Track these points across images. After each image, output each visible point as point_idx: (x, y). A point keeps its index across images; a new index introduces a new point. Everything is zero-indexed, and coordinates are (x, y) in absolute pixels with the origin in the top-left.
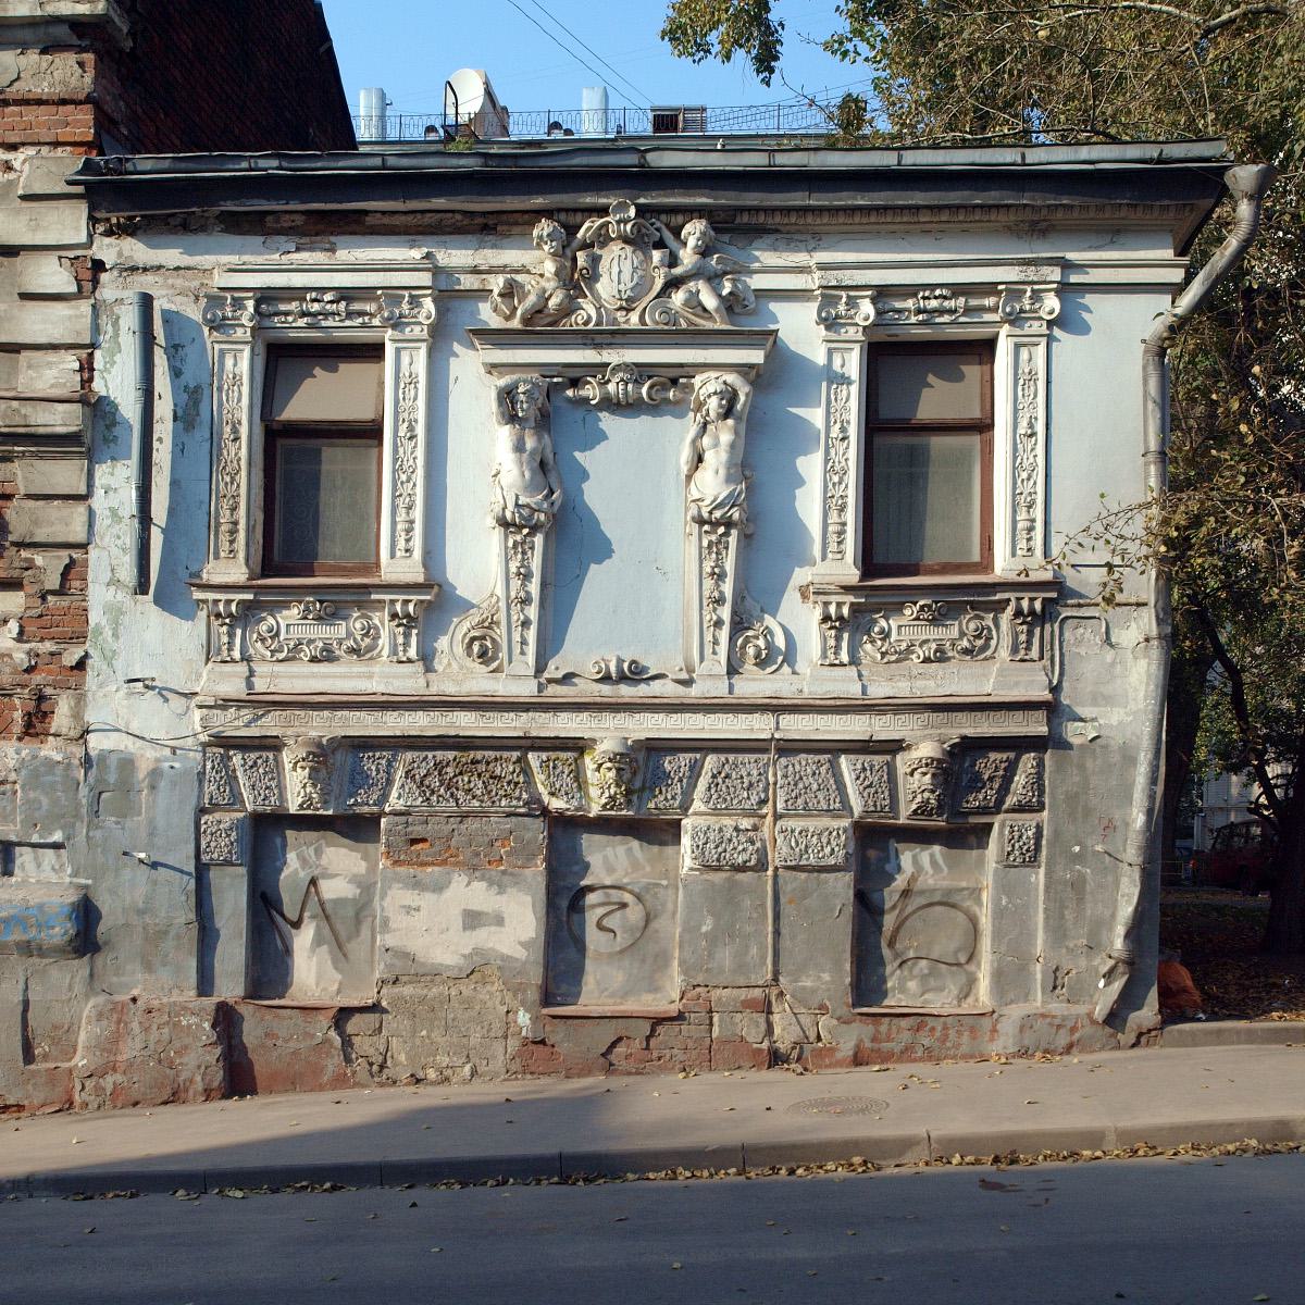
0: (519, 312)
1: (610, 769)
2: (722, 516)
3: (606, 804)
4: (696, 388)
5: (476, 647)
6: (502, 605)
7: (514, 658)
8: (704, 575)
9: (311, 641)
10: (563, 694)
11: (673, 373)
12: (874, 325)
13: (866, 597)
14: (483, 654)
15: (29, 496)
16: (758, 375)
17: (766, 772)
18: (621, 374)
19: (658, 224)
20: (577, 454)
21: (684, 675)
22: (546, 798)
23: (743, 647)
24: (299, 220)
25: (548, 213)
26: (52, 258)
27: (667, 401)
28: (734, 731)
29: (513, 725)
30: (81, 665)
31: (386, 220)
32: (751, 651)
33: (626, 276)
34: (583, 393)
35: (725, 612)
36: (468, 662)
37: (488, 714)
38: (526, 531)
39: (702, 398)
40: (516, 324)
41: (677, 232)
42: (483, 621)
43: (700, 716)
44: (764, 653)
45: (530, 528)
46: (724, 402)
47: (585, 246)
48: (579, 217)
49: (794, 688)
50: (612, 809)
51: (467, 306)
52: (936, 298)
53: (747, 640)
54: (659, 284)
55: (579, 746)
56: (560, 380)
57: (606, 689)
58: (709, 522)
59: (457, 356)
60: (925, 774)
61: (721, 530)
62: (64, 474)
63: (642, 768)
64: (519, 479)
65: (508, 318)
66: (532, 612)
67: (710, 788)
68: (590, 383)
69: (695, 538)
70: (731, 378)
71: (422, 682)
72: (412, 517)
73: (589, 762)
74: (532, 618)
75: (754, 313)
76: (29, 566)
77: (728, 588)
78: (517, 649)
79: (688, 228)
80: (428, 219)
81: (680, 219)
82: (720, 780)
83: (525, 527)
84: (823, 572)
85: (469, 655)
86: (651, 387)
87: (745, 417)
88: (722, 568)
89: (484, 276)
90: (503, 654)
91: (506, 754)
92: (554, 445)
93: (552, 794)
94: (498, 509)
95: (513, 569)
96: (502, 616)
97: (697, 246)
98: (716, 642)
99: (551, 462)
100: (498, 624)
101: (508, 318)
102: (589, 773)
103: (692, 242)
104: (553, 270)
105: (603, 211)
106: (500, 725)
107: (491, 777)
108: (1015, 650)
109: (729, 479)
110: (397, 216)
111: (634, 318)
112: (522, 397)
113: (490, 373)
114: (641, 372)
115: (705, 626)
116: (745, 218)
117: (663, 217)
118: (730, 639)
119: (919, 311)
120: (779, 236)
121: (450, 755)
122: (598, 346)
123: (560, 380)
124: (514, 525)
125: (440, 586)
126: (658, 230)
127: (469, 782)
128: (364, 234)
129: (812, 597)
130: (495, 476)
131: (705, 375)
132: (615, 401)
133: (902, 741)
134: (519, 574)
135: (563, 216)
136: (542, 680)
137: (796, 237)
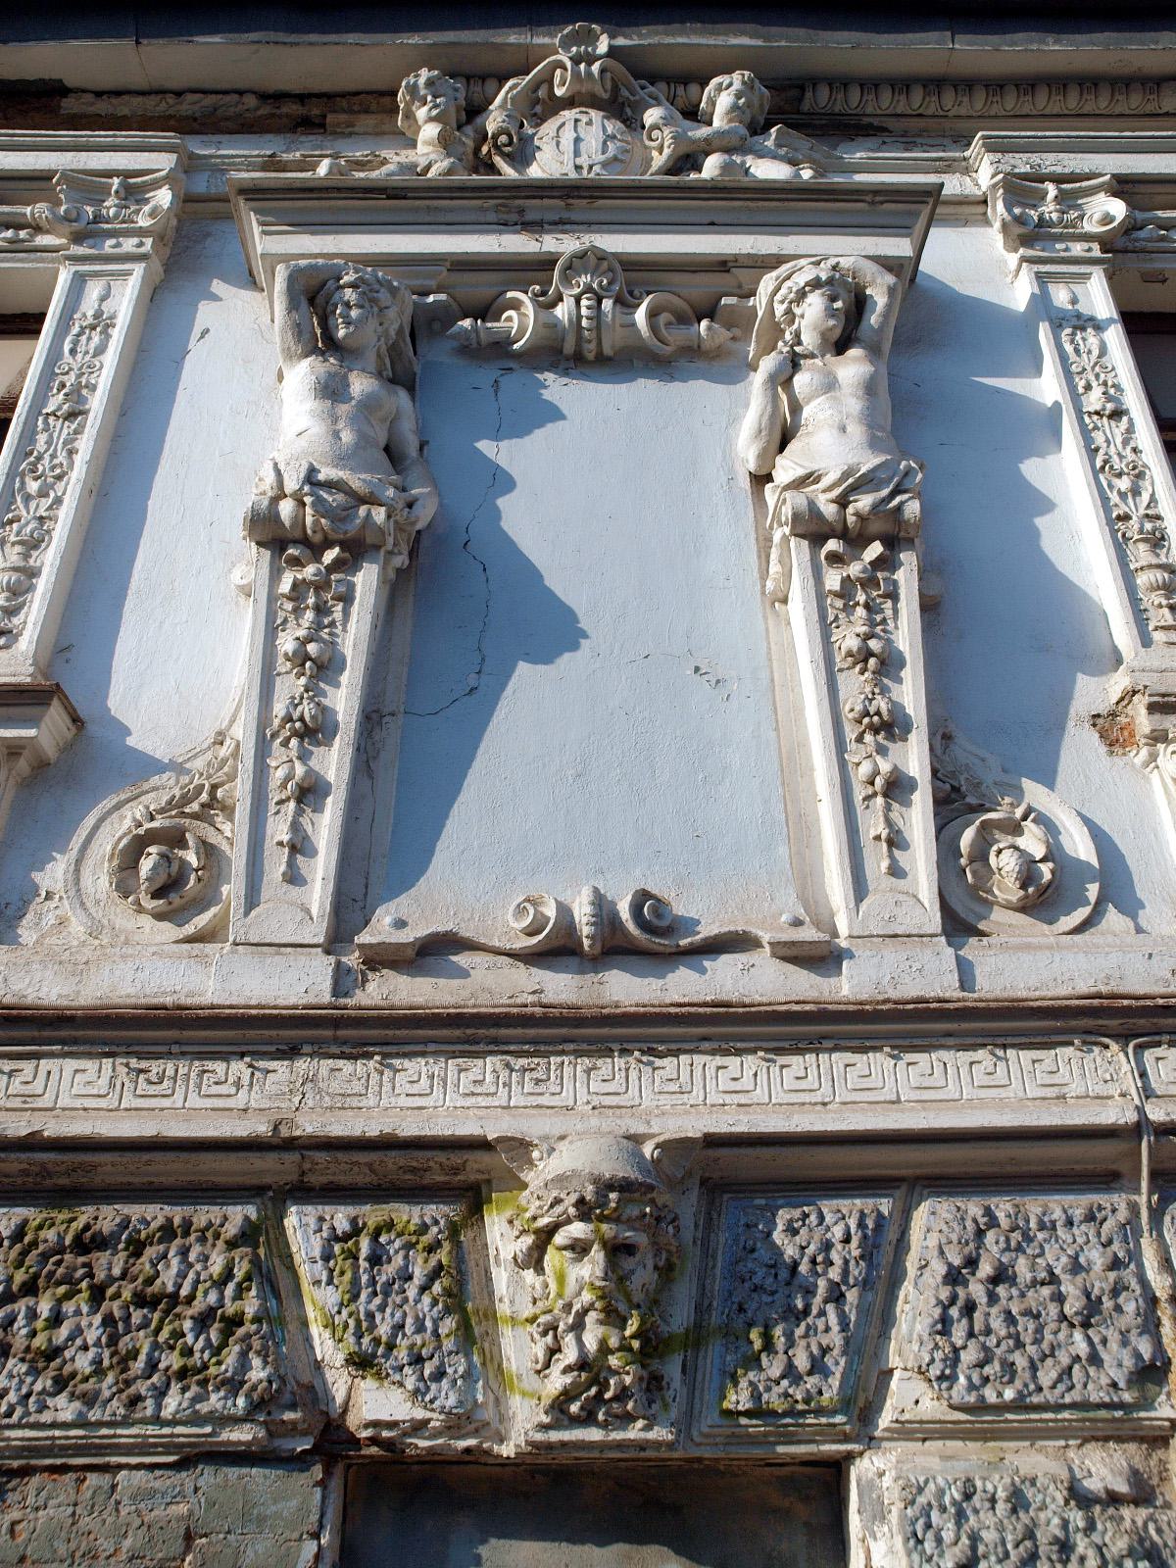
1: (579, 1249)
2: (875, 507)
3: (567, 1395)
7: (265, 893)
8: (839, 661)
11: (699, 287)
14: (167, 887)
17: (1135, 1255)
18: (584, 279)
20: (485, 446)
22: (339, 1383)
23: (980, 855)
28: (1001, 1104)
31: (102, 107)
35: (914, 757)
36: (122, 916)
37: (155, 1067)
38: (330, 556)
42: (186, 799)
43: (878, 1063)
44: (1046, 870)
45: (344, 545)
46: (839, 304)
50: (587, 1419)
56: (443, 297)
57: (560, 987)
59: (216, 298)
61: (875, 550)
63: (694, 1253)
66: (334, 762)
67: (944, 1326)
68: (516, 305)
74: (331, 776)
77: (910, 693)
78: (276, 865)
82: (977, 1290)
83: (328, 544)
85: (124, 889)
87: (887, 346)
90: (232, 890)
91: (204, 1215)
92: (421, 430)
93: (362, 1363)
95: (286, 644)
96: (240, 791)
97: (735, 107)
98: (895, 841)
99: (412, 449)
106: (194, 1101)
107: (140, 1300)
110: (126, 97)
112: (349, 294)
114: (635, 276)
115: (859, 793)
118: (939, 830)
120: (887, 140)
123: (443, 297)
124: (304, 541)
127: (56, 1320)
132: (569, 347)
134: (300, 658)
136: (352, 960)
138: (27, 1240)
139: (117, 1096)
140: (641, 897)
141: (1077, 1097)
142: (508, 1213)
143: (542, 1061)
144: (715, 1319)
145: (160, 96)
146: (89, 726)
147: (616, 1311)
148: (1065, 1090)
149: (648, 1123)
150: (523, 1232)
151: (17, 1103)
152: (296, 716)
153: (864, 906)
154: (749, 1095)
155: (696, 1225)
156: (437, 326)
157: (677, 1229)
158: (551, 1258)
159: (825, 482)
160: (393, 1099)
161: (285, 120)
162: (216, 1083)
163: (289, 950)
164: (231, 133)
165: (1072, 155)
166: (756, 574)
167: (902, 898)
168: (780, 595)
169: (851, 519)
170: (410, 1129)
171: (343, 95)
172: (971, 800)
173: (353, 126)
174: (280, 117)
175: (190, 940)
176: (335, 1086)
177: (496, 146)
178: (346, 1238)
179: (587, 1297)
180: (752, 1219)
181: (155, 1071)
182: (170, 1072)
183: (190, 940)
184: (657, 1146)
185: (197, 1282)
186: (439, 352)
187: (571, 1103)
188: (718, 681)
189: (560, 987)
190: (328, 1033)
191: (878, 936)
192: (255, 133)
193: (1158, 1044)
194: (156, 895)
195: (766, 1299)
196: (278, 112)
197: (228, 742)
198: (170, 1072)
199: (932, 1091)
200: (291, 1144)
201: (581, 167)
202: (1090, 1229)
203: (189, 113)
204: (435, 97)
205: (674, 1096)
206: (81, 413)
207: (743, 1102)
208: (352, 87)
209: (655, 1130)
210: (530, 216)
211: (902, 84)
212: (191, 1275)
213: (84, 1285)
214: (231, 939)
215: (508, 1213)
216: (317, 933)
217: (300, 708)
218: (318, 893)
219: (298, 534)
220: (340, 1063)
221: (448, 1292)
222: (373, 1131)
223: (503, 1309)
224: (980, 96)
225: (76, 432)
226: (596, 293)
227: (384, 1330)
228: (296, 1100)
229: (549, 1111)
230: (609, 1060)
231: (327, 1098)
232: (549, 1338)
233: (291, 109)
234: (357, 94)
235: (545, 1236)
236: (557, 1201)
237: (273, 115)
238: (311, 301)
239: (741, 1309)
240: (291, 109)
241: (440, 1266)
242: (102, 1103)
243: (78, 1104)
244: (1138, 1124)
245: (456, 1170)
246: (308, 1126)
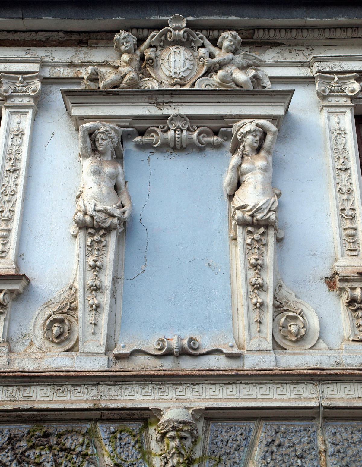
5: (55, 330)
10: (130, 369)
11: (215, 124)
21: (236, 351)
28: (283, 400)
29: (85, 398)
31: (11, 37)
39: (239, 138)
42: (63, 308)
48: (145, 32)
49: (333, 361)
56: (131, 129)
57: (168, 364)
66: (104, 300)
70: (261, 122)
72: (10, 228)
73: (153, 434)
81: (216, 33)
86: (199, 134)
89: (77, 69)
91: (76, 426)
100: (75, 309)
102: (153, 444)
106: (73, 398)
107: (62, 450)
110: (18, 33)
116: (260, 34)
120: (284, 48)
121: (24, 428)
122: (160, 105)
123: (131, 129)
125: (28, 280)
126: (201, 38)
127: (41, 455)
129: (339, 284)
130: (78, 197)
132: (172, 145)
136: (112, 357)
137: (295, 48)
138: (31, 434)
139: (52, 396)
140: (191, 339)
141: (304, 398)
142: (155, 427)
143: (163, 386)
144: (207, 454)
145: (30, 33)
146: (32, 282)
147: (182, 453)
148: (301, 396)
149: (191, 404)
150: (158, 433)
151: (26, 399)
152: (94, 284)
153: (251, 342)
154: (217, 396)
155: (203, 430)
156: (129, 136)
157: (198, 432)
158: (166, 440)
159: (248, 208)
160: (124, 397)
161: (74, 41)
162: (78, 393)
163: (95, 354)
164: (56, 46)
165: (345, 62)
166: (228, 231)
167: (262, 339)
168: (235, 238)
169: (255, 221)
170: (130, 406)
171: (94, 32)
172: (285, 308)
173: (97, 44)
174: (72, 40)
175: (67, 351)
176: (110, 393)
177: (147, 63)
178: (113, 433)
179: (174, 450)
180: (217, 428)
181: (62, 389)
182: (66, 390)
183: (67, 351)
184: (193, 411)
185: (76, 445)
186: (130, 146)
187: (171, 398)
188: (215, 268)
189: (168, 364)
190: (107, 379)
191: (255, 350)
192: (64, 46)
193: (328, 383)
194: (57, 338)
195: (220, 450)
196: (71, 38)
197: (73, 288)
198: (66, 390)
199: (265, 396)
200: (98, 409)
201: (176, 73)
202: (305, 432)
203: (40, 39)
204: (127, 42)
205: (198, 396)
206: (18, 170)
207: (216, 398)
208: (97, 29)
209: (192, 406)
210: (159, 101)
211: (289, 29)
212: (74, 443)
213: (47, 446)
214: (79, 351)
215: (155, 427)
216: (102, 349)
217: (95, 282)
218: (102, 338)
219: (91, 226)
220: (110, 387)
221: (140, 447)
222: (120, 406)
223: (153, 451)
224: (316, 32)
225: (17, 177)
226: (180, 129)
227: (124, 457)
228: (99, 397)
229: (165, 400)
230: (181, 386)
231: (107, 397)
232: (165, 460)
233: (75, 37)
234: (99, 32)
235: (163, 435)
236: (167, 426)
237: (70, 40)
238: (90, 135)
239: (214, 452)
240: (75, 37)
241: (137, 440)
242: (48, 399)
243: (42, 399)
244: (319, 406)
245: (141, 415)
246: (103, 405)
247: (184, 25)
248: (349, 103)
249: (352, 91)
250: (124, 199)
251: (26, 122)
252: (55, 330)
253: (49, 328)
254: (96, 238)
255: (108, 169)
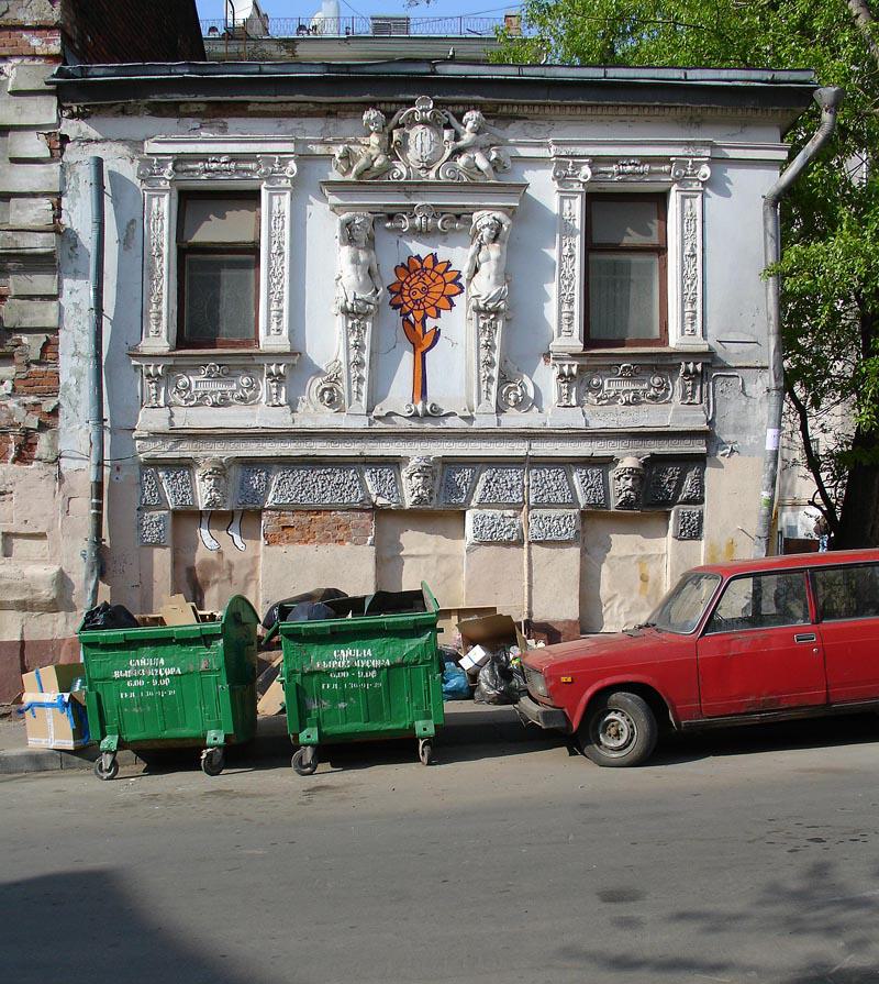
0: (354, 170)
4: (474, 222)
5: (326, 396)
6: (344, 367)
9: (212, 393)
11: (459, 211)
12: (591, 181)
13: (588, 361)
15: (17, 297)
16: (514, 213)
17: (523, 478)
19: (447, 113)
23: (507, 394)
24: (203, 108)
25: (373, 105)
26: (33, 134)
27: (454, 229)
30: (55, 412)
31: (262, 108)
32: (512, 397)
33: (426, 147)
34: (398, 225)
35: (495, 372)
36: (321, 406)
40: (351, 177)
41: (459, 117)
47: (398, 126)
51: (319, 165)
52: (630, 164)
53: (510, 389)
54: (448, 152)
55: (395, 463)
58: (485, 311)
60: (627, 479)
61: (492, 316)
62: (42, 283)
63: (439, 476)
64: (356, 283)
65: (344, 174)
66: (365, 372)
67: (485, 490)
69: (474, 322)
70: (498, 215)
71: (289, 418)
72: (280, 308)
75: (508, 172)
76: (19, 343)
77: (496, 356)
79: (468, 115)
80: (290, 107)
81: (461, 109)
82: (492, 484)
84: (558, 344)
88: (493, 341)
93: (378, 495)
94: (341, 302)
96: (343, 374)
99: (376, 270)
101: (344, 174)
103: (470, 124)
104: (377, 142)
105: (411, 103)
108: (684, 397)
109: (497, 283)
111: (432, 174)
113: (333, 210)
114: (437, 211)
117: (450, 108)
119: (620, 173)
122: (408, 194)
128: (246, 117)
130: (337, 280)
131: (481, 213)
133: (613, 457)
135: (383, 106)
136: (372, 417)
164: (306, 117)
240: (325, 108)
247: (431, 106)
248: (581, 189)
249: (586, 177)
250: (377, 280)
251: (285, 203)
252: (326, 396)
253: (322, 394)
254: (355, 321)
255: (363, 256)
